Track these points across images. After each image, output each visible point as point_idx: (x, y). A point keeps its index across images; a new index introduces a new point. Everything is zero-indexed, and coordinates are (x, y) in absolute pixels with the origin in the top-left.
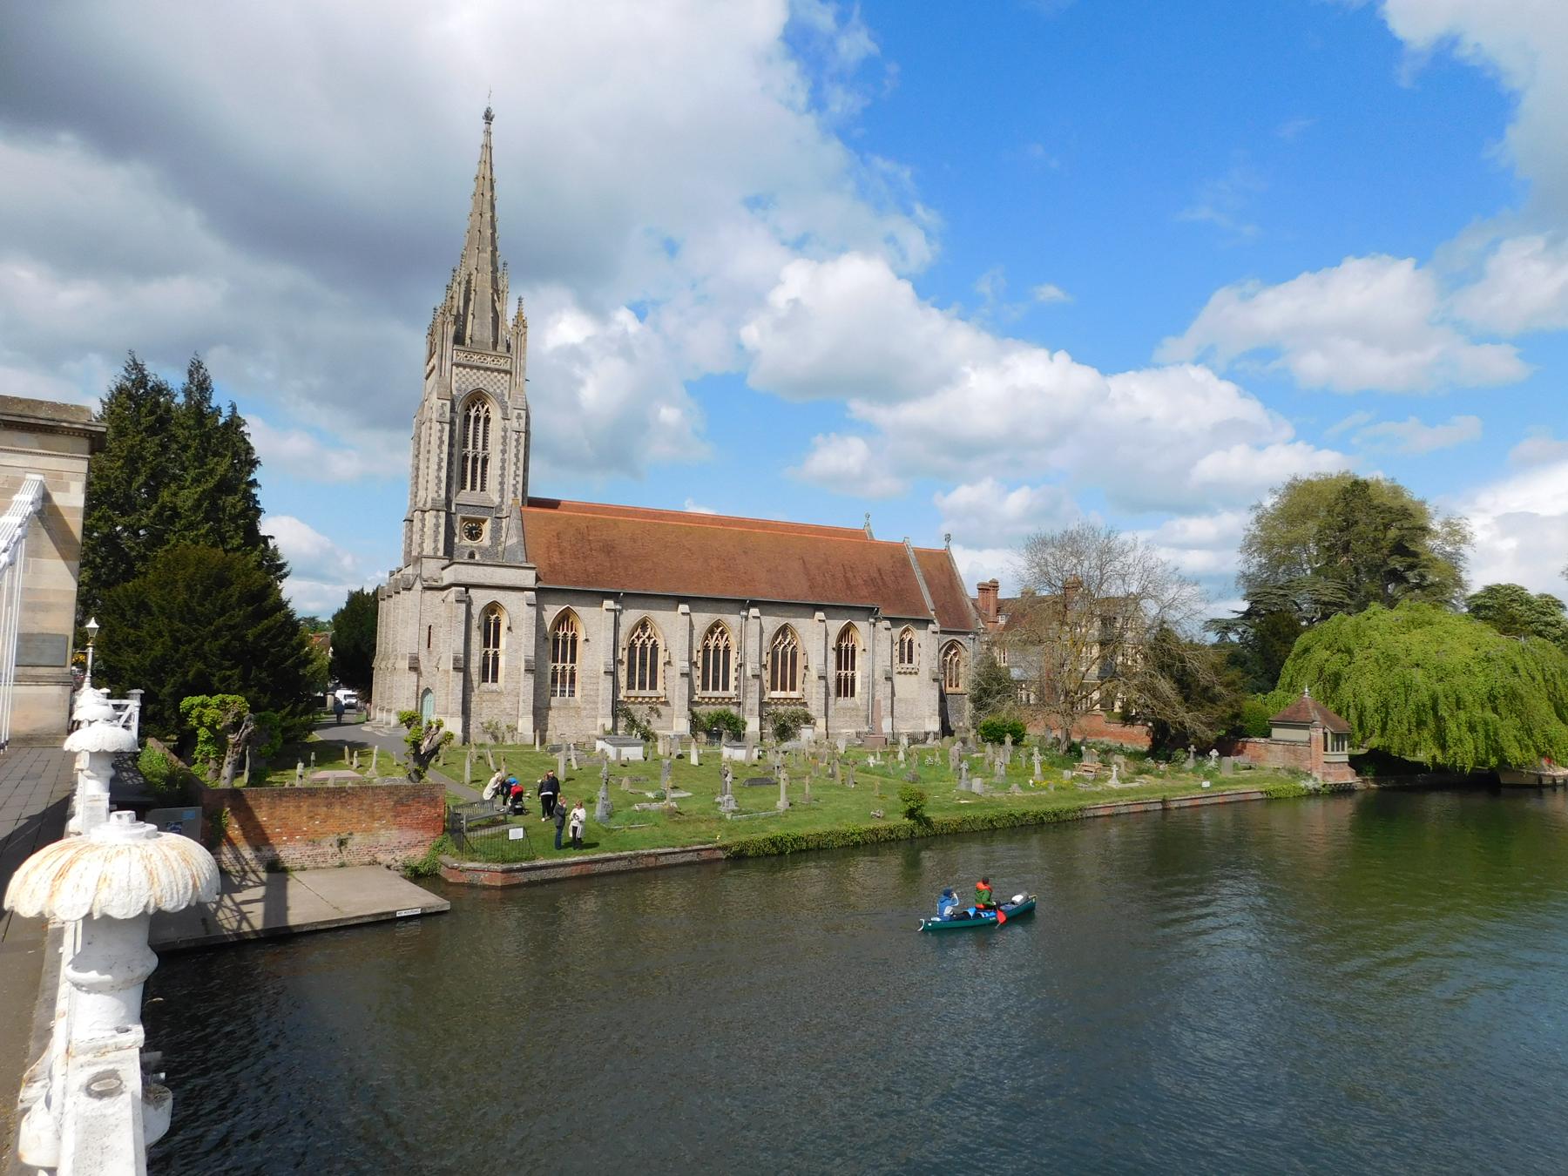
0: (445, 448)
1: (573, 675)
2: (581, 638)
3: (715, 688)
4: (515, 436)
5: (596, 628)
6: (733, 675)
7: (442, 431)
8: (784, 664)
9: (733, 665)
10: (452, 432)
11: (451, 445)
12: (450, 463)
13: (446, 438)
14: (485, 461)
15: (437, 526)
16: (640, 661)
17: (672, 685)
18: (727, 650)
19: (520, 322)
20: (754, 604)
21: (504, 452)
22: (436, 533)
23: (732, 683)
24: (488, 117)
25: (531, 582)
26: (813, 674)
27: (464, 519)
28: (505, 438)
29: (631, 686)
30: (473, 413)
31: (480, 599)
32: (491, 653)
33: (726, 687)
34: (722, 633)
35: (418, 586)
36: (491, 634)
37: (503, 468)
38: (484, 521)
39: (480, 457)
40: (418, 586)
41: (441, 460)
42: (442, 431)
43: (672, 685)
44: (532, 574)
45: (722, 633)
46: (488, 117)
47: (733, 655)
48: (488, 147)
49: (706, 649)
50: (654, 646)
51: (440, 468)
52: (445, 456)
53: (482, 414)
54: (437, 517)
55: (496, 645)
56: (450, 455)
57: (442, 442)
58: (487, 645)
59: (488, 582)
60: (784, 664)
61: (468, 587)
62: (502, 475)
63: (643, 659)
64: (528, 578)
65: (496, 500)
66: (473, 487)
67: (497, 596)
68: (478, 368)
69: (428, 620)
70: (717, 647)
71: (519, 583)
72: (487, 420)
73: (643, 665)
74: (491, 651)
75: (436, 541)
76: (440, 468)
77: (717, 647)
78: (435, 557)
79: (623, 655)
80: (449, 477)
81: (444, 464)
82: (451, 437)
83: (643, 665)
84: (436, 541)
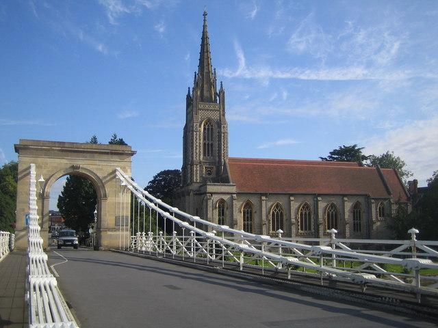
1: (251, 225)
2: (254, 211)
8: (332, 219)
11: (200, 140)
14: (212, 145)
19: (222, 91)
20: (319, 195)
21: (219, 141)
22: (196, 173)
23: (312, 227)
24: (205, 15)
30: (207, 128)
31: (216, 198)
33: (310, 229)
34: (307, 208)
39: (210, 143)
40: (191, 193)
45: (307, 208)
46: (205, 15)
48: (204, 26)
50: (281, 213)
51: (196, 149)
54: (196, 167)
55: (223, 215)
56: (200, 143)
59: (219, 191)
60: (332, 219)
62: (219, 150)
63: (277, 219)
68: (208, 110)
71: (230, 191)
73: (277, 221)
75: (196, 176)
76: (196, 149)
84: (196, 176)
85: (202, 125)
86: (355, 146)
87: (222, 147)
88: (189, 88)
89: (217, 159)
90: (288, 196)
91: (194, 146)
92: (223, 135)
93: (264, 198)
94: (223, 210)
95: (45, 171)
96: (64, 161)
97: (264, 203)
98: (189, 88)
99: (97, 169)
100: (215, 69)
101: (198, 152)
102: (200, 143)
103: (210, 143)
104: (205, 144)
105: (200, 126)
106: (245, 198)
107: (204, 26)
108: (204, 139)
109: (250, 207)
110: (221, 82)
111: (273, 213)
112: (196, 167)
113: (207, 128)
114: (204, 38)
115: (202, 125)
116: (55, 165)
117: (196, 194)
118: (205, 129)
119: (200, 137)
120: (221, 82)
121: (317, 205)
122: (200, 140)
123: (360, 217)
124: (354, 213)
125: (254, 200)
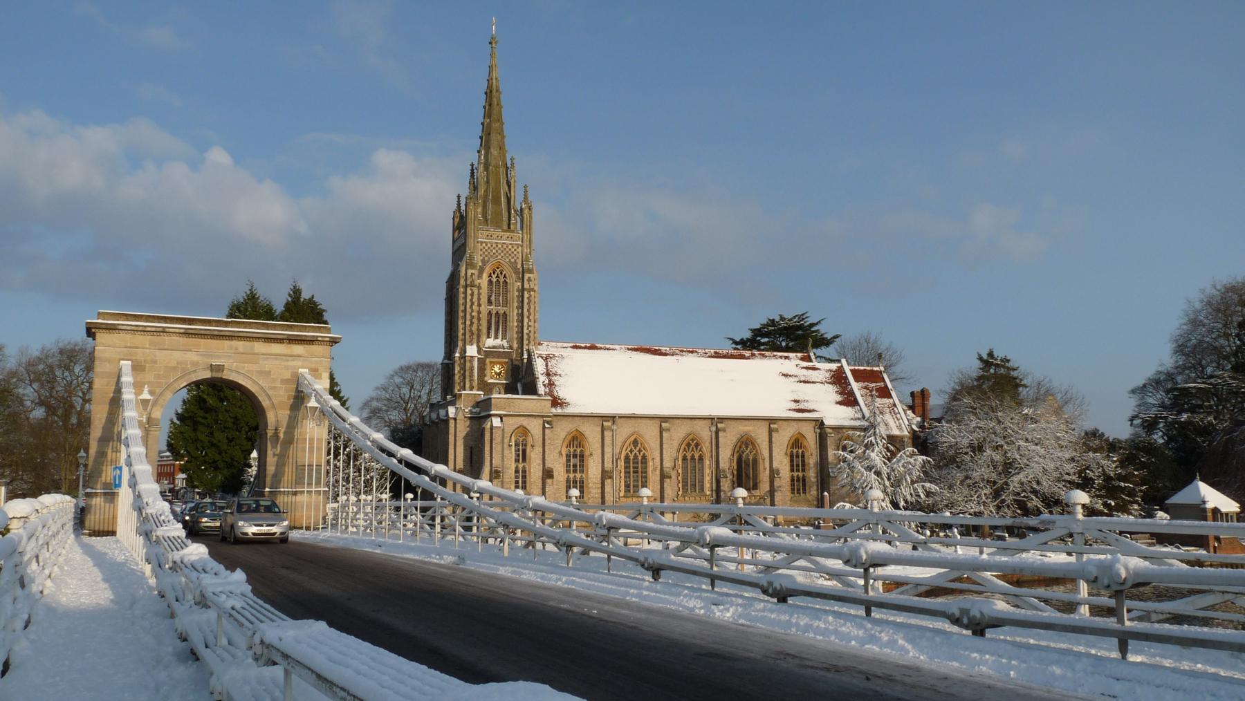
2: (587, 453)
7: (472, 295)
10: (479, 294)
11: (479, 305)
13: (475, 299)
18: (701, 459)
30: (494, 280)
31: (512, 423)
32: (520, 466)
34: (697, 445)
36: (522, 456)
41: (472, 317)
42: (472, 295)
45: (697, 445)
50: (644, 457)
51: (472, 323)
52: (474, 314)
53: (502, 280)
55: (524, 460)
56: (479, 312)
57: (473, 303)
58: (517, 461)
66: (496, 337)
67: (524, 422)
70: (693, 458)
74: (520, 466)
76: (472, 323)
77: (693, 458)
79: (621, 464)
80: (479, 330)
81: (475, 321)
82: (479, 299)
85: (485, 275)
86: (801, 317)
87: (526, 320)
88: (459, 197)
90: (658, 422)
91: (468, 317)
92: (526, 295)
94: (524, 452)
95: (149, 376)
96: (192, 357)
97: (608, 434)
98: (459, 197)
99: (261, 373)
102: (479, 312)
103: (501, 312)
104: (490, 313)
105: (480, 276)
110: (525, 187)
111: (627, 458)
113: (494, 280)
115: (485, 275)
116: (174, 364)
118: (490, 282)
119: (479, 299)
120: (525, 187)
121: (717, 438)
122: (479, 305)
123: (803, 465)
124: (792, 456)
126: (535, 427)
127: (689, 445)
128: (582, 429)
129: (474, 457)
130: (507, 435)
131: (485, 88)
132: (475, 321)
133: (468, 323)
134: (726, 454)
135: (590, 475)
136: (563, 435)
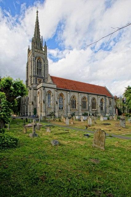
0: (35, 66)
2: (64, 99)
3: (85, 108)
4: (46, 65)
5: (67, 97)
6: (87, 106)
7: (34, 63)
9: (87, 105)
12: (35, 69)
14: (41, 70)
15: (34, 80)
16: (73, 103)
17: (79, 106)
21: (44, 68)
25: (55, 87)
26: (98, 106)
27: (38, 79)
28: (44, 66)
29: (72, 107)
30: (38, 61)
31: (47, 90)
33: (86, 108)
35: (32, 89)
36: (49, 98)
37: (44, 71)
38: (41, 80)
42: (34, 63)
43: (79, 106)
44: (56, 86)
47: (87, 103)
48: (37, 17)
49: (83, 101)
51: (34, 69)
52: (35, 67)
54: (34, 78)
55: (50, 99)
56: (35, 68)
59: (48, 86)
61: (44, 87)
63: (74, 103)
64: (55, 86)
65: (43, 77)
67: (50, 89)
69: (35, 95)
72: (41, 63)
73: (74, 104)
78: (34, 84)
81: (35, 69)
83: (74, 104)
89: (43, 77)
90: (78, 93)
92: (46, 65)
93: (68, 92)
97: (69, 95)
100: (42, 36)
101: (34, 71)
104: (37, 69)
106: (60, 92)
107: (37, 17)
108: (37, 67)
109: (62, 96)
112: (34, 78)
113: (38, 61)
114: (37, 23)
117: (35, 89)
118: (38, 62)
125: (64, 93)
126: (52, 90)
127: (84, 99)
128: (63, 93)
129: (36, 99)
130: (46, 92)
131: (35, 21)
132: (35, 69)
133: (33, 69)
134: (90, 101)
135: (65, 104)
136: (59, 94)
